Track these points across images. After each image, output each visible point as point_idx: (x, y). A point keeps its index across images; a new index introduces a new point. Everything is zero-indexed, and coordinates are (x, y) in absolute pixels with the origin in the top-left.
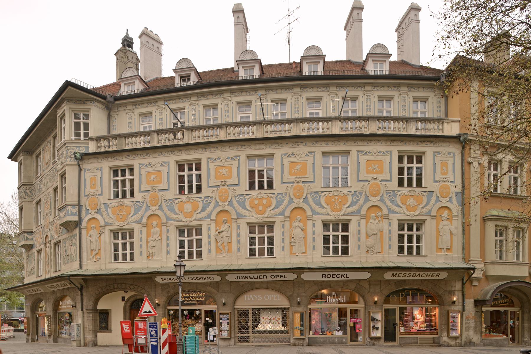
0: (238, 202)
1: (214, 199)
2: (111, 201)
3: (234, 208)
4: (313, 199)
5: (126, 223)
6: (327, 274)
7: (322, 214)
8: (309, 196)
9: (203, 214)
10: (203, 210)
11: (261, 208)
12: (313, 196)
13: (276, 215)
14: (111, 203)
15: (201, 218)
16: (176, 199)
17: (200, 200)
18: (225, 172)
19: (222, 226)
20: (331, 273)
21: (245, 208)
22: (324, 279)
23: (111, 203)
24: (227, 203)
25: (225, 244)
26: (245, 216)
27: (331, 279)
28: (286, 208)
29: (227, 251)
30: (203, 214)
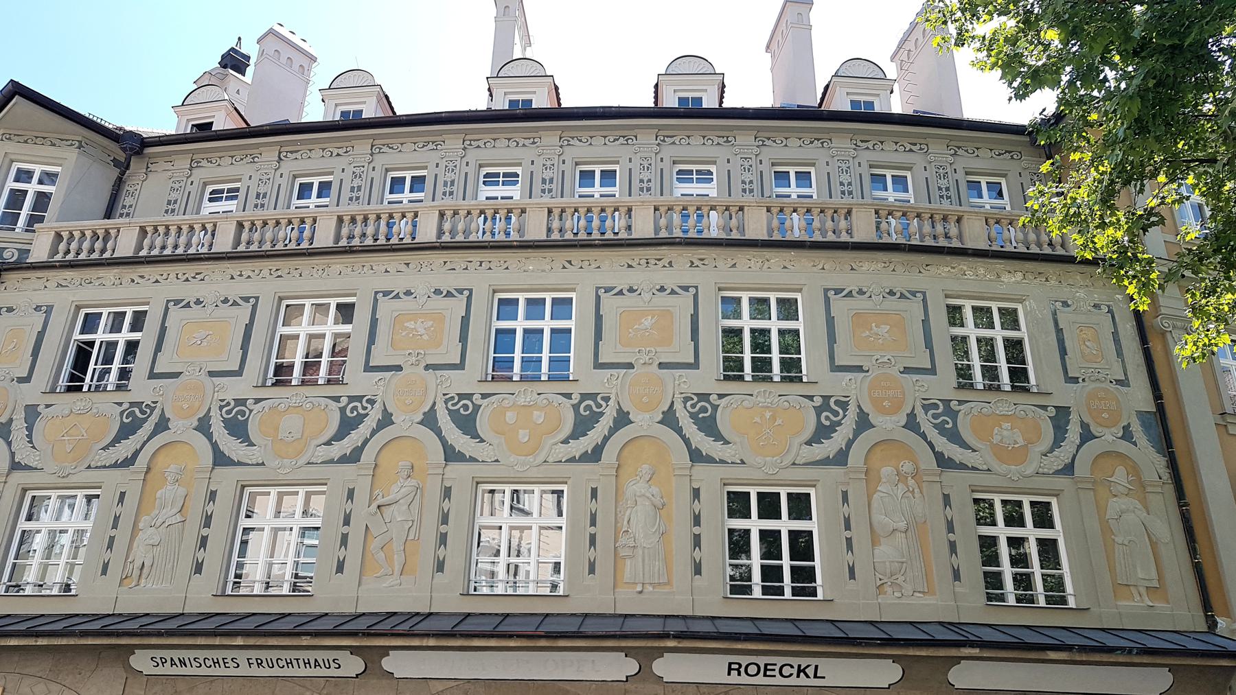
0: (454, 415)
1: (377, 406)
2: (50, 399)
3: (438, 433)
4: (692, 416)
5: (82, 468)
6: (744, 660)
7: (722, 462)
8: (678, 406)
9: (337, 449)
10: (339, 436)
11: (523, 435)
12: (693, 406)
13: (572, 460)
14: (48, 406)
15: (331, 461)
16: (257, 401)
17: (333, 405)
18: (421, 331)
19: (395, 488)
20: (762, 661)
21: (475, 435)
22: (734, 678)
23: (48, 406)
24: (420, 417)
25: (397, 546)
26: (473, 460)
27: (760, 679)
28: (606, 439)
29: (397, 568)
30: (337, 449)
